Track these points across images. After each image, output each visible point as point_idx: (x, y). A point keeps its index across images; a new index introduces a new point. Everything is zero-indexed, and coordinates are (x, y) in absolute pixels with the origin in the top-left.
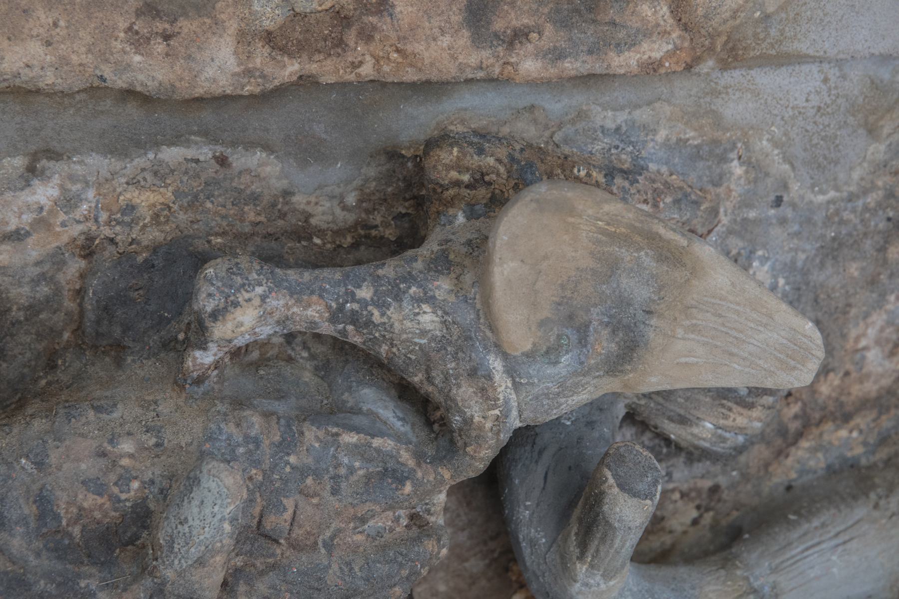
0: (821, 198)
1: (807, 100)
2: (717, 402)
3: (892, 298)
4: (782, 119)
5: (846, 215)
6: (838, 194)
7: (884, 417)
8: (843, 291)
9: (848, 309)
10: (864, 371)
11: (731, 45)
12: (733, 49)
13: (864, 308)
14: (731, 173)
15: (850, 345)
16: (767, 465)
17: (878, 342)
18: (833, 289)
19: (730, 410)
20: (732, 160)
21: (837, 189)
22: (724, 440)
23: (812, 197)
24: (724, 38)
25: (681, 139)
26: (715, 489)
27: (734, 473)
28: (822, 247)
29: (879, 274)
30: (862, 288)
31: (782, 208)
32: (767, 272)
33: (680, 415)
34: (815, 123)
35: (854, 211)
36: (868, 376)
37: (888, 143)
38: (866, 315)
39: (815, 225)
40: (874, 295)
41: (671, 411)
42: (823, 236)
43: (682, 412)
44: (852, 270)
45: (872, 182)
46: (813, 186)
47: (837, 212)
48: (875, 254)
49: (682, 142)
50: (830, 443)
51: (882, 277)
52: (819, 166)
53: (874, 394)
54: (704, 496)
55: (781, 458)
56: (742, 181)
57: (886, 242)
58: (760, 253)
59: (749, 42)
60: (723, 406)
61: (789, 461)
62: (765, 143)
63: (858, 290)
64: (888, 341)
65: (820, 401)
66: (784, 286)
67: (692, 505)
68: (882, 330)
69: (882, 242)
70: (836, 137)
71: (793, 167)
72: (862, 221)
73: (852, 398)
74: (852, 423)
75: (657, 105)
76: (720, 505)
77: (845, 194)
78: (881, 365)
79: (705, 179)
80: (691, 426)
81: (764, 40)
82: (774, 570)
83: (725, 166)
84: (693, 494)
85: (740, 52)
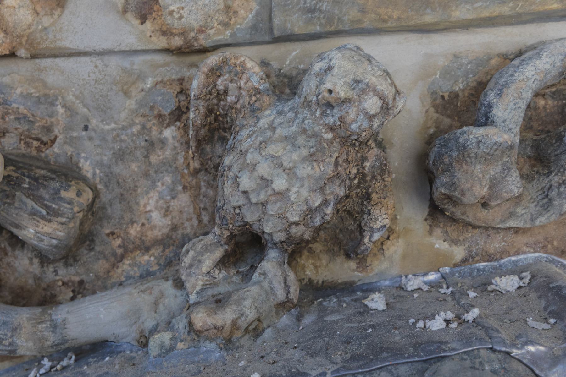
0: (107, 127)
1: (89, 76)
2: (31, 217)
3: (159, 184)
4: (78, 85)
5: (123, 137)
6: (116, 126)
7: (167, 250)
8: (131, 178)
9: (136, 188)
10: (152, 223)
11: (29, 42)
12: (31, 44)
13: (145, 189)
14: (58, 112)
15: (141, 208)
16: (109, 272)
17: (156, 208)
18: (125, 177)
19: (38, 222)
20: (57, 105)
21: (115, 123)
22: (42, 240)
23: (102, 126)
24: (25, 38)
25: (28, 93)
26: (81, 282)
27: (91, 275)
28: (114, 153)
29: (149, 171)
30: (141, 177)
31: (88, 131)
32: (89, 165)
33: (15, 223)
34: (95, 88)
35: (127, 135)
36: (155, 226)
37: (135, 99)
38: (147, 193)
39: (107, 141)
40: (149, 182)
41: (10, 220)
42: (113, 148)
43: (17, 222)
44: (133, 167)
45: (132, 120)
46: (102, 121)
47: (118, 135)
48: (143, 159)
49: (29, 96)
50: (140, 263)
51: (150, 172)
52: (102, 110)
53: (160, 237)
54: (76, 285)
55: (115, 269)
56: (64, 116)
57: (148, 153)
58: (83, 155)
59: (39, 40)
60: (34, 219)
61: (119, 270)
62: (71, 97)
63: (139, 179)
64: (162, 208)
65: (132, 238)
66: (100, 173)
67: (70, 290)
68: (157, 202)
69: (146, 153)
70: (107, 95)
71: (88, 109)
72: (132, 140)
73: (149, 238)
74: (151, 252)
75: (12, 75)
76: (85, 291)
77: (121, 126)
78: (160, 221)
79: (44, 114)
80: (21, 229)
81: (46, 40)
82: (68, 312)
83: (54, 108)
84: (70, 284)
85: (35, 45)
